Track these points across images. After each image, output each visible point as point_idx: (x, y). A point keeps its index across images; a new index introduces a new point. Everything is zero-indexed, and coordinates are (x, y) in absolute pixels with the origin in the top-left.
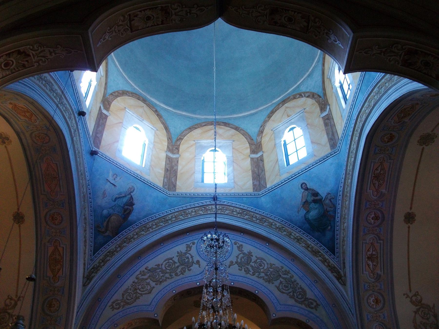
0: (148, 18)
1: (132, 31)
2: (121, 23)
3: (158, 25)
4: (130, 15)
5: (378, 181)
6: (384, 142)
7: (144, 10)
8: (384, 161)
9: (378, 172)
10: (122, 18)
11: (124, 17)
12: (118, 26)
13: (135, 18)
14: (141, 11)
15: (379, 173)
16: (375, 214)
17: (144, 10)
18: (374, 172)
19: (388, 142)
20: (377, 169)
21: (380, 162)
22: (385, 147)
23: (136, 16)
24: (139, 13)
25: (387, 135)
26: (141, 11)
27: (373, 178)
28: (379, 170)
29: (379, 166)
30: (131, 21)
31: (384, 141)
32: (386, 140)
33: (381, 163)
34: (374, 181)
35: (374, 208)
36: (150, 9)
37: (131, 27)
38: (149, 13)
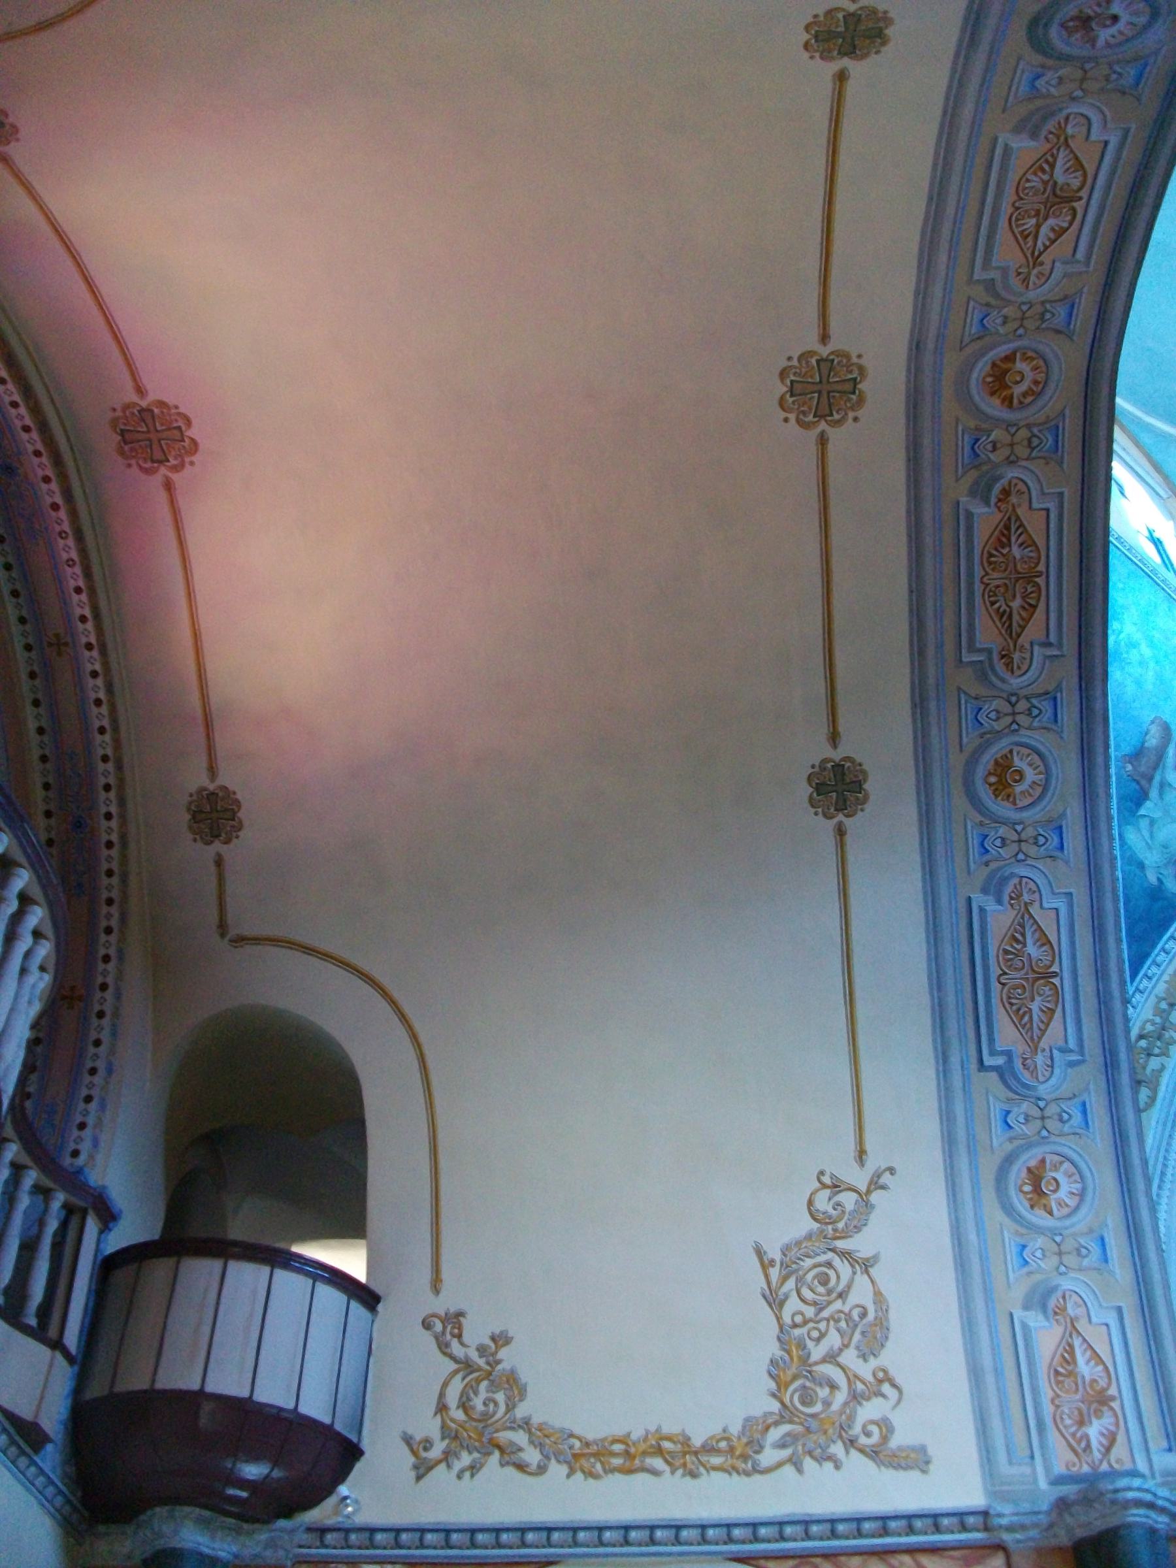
5: (1055, 183)
6: (1030, 354)
8: (1019, 274)
9: (1051, 222)
15: (1046, 219)
16: (1093, 41)
18: (1071, 224)
19: (1010, 358)
20: (1060, 232)
21: (1042, 264)
22: (1021, 331)
25: (1025, 395)
27: (1084, 194)
28: (1044, 230)
29: (1046, 248)
31: (1032, 359)
32: (1020, 365)
33: (1036, 261)
34: (1076, 183)
35: (1088, 66)
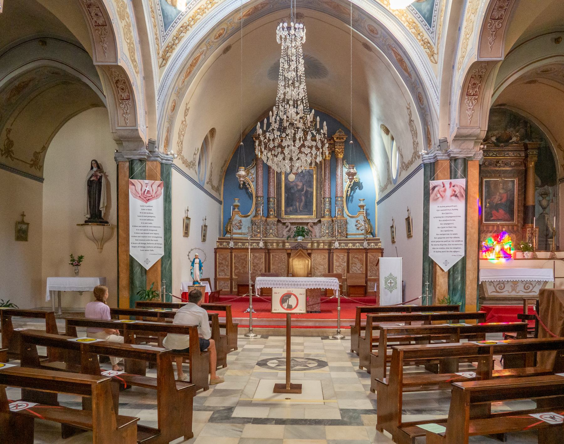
0: (96, 15)
1: (106, 25)
2: (100, 33)
3: (100, 10)
4: (95, 26)
7: (92, 17)
10: (97, 31)
11: (97, 29)
12: (101, 35)
13: (97, 22)
14: (93, 19)
17: (92, 17)
23: (96, 22)
24: (94, 20)
26: (93, 19)
30: (99, 25)
36: (90, 13)
37: (103, 26)
38: (93, 14)
